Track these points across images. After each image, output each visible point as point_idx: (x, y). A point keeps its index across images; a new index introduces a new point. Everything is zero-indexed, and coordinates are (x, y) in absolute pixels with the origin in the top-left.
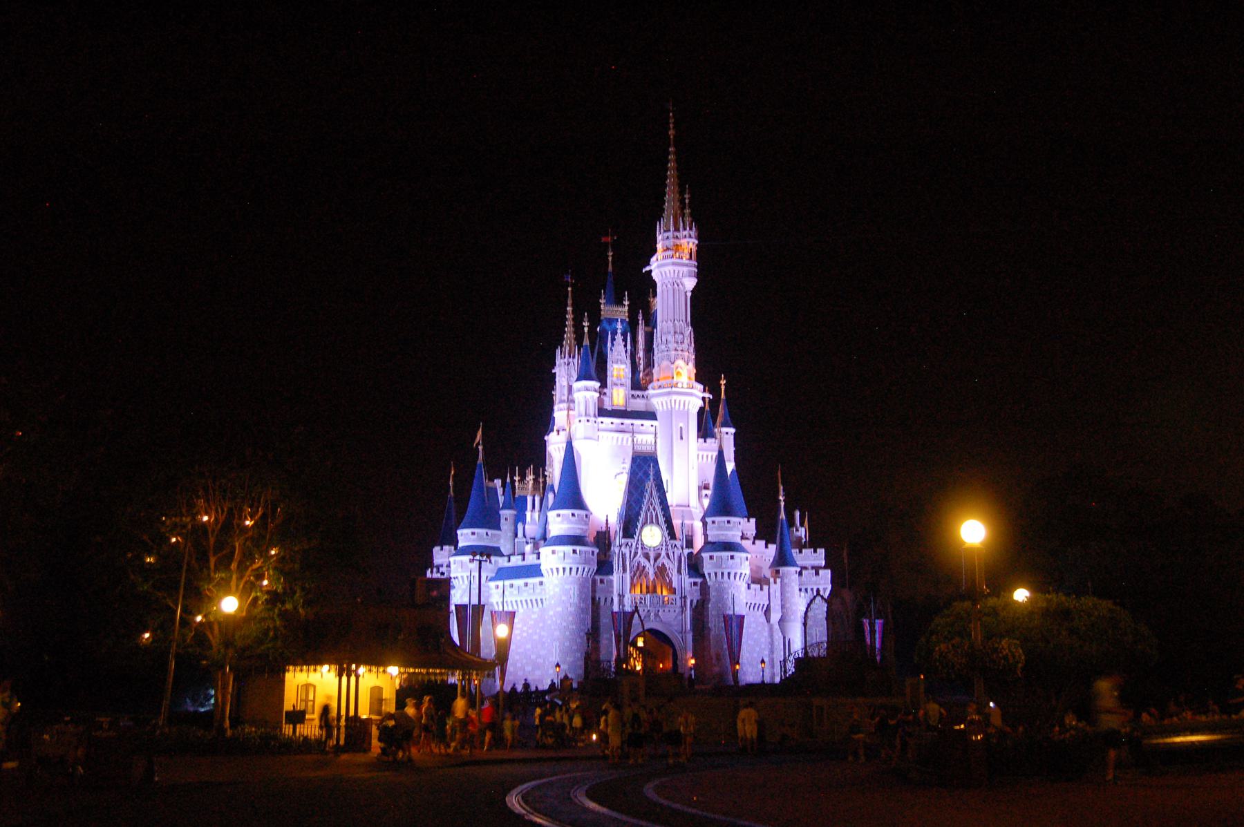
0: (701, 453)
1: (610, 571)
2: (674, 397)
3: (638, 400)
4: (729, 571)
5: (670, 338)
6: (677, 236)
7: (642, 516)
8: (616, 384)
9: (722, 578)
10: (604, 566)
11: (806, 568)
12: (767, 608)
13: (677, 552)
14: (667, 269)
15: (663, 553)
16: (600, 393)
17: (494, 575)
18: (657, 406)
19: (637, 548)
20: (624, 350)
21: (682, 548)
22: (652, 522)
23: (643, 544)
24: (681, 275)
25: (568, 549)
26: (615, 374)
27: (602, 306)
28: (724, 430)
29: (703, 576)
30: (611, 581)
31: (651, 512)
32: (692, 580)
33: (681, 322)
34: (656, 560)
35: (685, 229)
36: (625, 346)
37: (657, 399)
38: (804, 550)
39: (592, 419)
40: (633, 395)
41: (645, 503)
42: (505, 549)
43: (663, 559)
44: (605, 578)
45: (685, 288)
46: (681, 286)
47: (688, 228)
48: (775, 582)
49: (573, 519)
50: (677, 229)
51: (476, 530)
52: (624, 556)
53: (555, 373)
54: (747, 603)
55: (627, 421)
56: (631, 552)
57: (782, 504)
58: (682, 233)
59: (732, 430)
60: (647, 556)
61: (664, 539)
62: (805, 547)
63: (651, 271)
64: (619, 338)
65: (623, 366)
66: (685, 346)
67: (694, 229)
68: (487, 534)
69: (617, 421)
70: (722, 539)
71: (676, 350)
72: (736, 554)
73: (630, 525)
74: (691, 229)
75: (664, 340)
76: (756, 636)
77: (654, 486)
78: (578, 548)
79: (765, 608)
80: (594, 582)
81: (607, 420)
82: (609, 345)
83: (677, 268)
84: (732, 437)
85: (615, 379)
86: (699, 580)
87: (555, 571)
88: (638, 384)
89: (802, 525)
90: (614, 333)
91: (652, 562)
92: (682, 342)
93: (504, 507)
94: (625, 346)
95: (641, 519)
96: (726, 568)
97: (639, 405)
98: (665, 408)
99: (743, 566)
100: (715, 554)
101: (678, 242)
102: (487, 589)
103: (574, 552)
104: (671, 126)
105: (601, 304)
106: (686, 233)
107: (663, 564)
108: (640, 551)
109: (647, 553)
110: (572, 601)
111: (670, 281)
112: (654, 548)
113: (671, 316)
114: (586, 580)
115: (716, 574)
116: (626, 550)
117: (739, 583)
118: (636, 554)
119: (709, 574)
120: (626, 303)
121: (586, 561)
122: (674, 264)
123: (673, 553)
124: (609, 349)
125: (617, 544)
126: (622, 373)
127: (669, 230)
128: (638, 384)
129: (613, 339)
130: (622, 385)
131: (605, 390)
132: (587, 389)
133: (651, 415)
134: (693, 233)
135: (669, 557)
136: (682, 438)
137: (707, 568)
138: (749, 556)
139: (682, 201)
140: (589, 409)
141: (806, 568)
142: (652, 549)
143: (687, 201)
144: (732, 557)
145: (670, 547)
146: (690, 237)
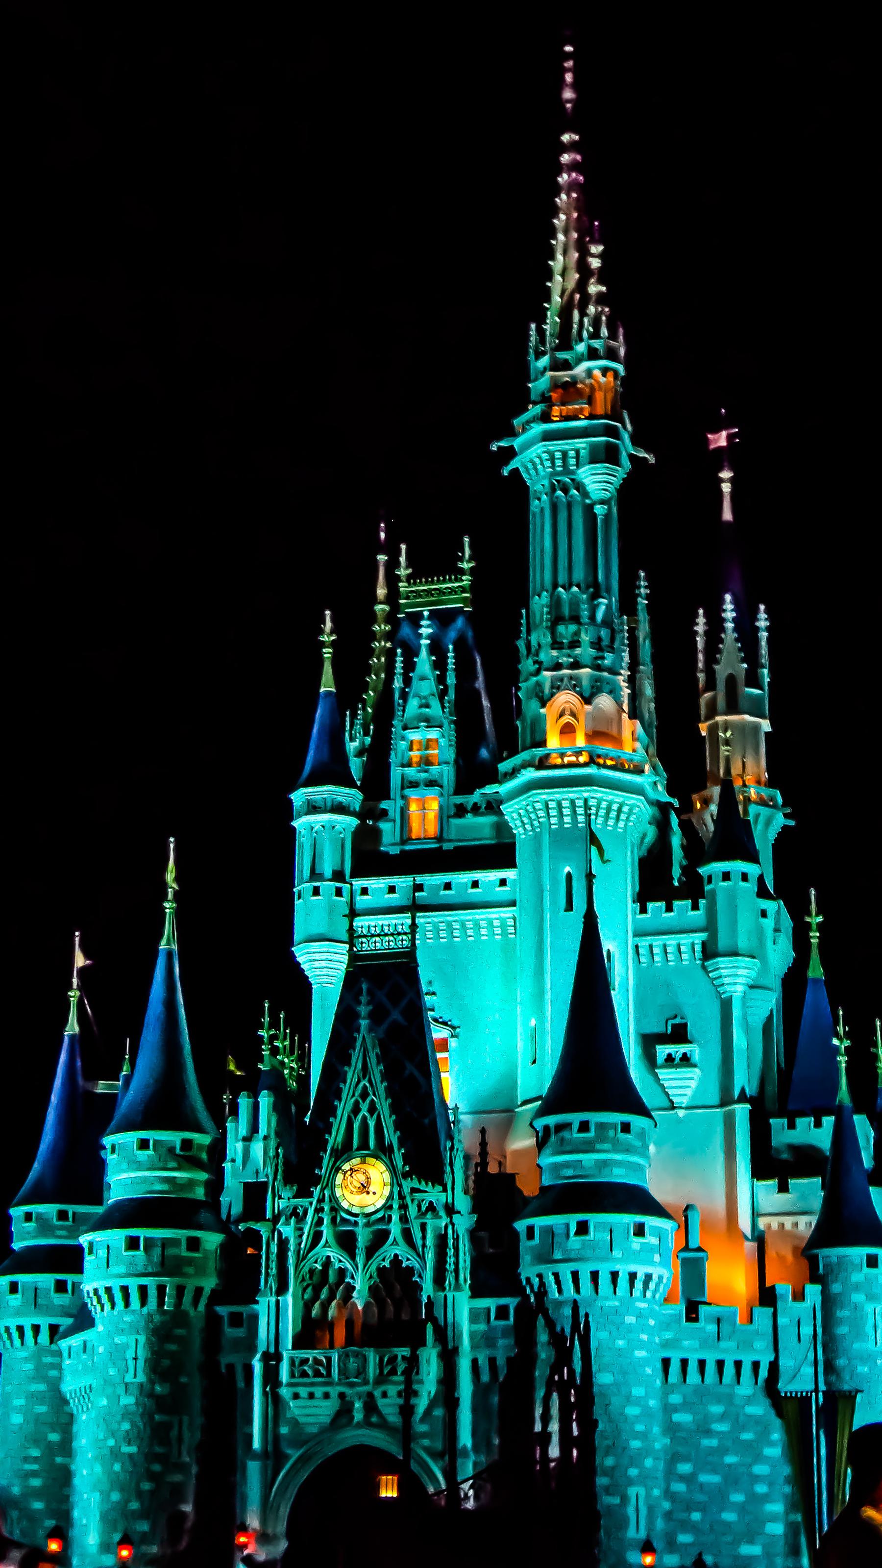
0: (644, 942)
1: (250, 1295)
2: (543, 795)
8: (414, 785)
9: (560, 1291)
12: (770, 1371)
15: (395, 1229)
17: (69, 1321)
23: (336, 1209)
24: (573, 461)
25: (117, 1236)
30: (255, 1318)
32: (490, 1303)
33: (575, 589)
34: (371, 1251)
39: (328, 887)
45: (585, 494)
46: (574, 492)
48: (799, 1296)
49: (144, 1155)
52: (283, 1244)
54: (666, 1362)
55: (432, 880)
56: (301, 1236)
60: (347, 1242)
61: (396, 1190)
65: (433, 734)
69: (403, 882)
71: (558, 667)
72: (594, 1219)
74: (613, 336)
76: (730, 1459)
79: (763, 1373)
80: (213, 1321)
81: (377, 884)
82: (398, 684)
85: (412, 772)
86: (512, 1302)
91: (360, 1259)
92: (575, 644)
94: (441, 680)
95: (335, 1138)
99: (617, 1253)
101: (564, 376)
102: (55, 1360)
103: (133, 1243)
104: (569, 77)
106: (581, 348)
107: (396, 1261)
108: (326, 1230)
110: (129, 1378)
111: (546, 482)
112: (368, 1215)
116: (287, 1230)
122: (548, 437)
123: (423, 1227)
125: (269, 1215)
129: (409, 666)
131: (384, 805)
132: (313, 808)
140: (322, 856)
142: (361, 1221)
145: (413, 1211)
146: (593, 354)
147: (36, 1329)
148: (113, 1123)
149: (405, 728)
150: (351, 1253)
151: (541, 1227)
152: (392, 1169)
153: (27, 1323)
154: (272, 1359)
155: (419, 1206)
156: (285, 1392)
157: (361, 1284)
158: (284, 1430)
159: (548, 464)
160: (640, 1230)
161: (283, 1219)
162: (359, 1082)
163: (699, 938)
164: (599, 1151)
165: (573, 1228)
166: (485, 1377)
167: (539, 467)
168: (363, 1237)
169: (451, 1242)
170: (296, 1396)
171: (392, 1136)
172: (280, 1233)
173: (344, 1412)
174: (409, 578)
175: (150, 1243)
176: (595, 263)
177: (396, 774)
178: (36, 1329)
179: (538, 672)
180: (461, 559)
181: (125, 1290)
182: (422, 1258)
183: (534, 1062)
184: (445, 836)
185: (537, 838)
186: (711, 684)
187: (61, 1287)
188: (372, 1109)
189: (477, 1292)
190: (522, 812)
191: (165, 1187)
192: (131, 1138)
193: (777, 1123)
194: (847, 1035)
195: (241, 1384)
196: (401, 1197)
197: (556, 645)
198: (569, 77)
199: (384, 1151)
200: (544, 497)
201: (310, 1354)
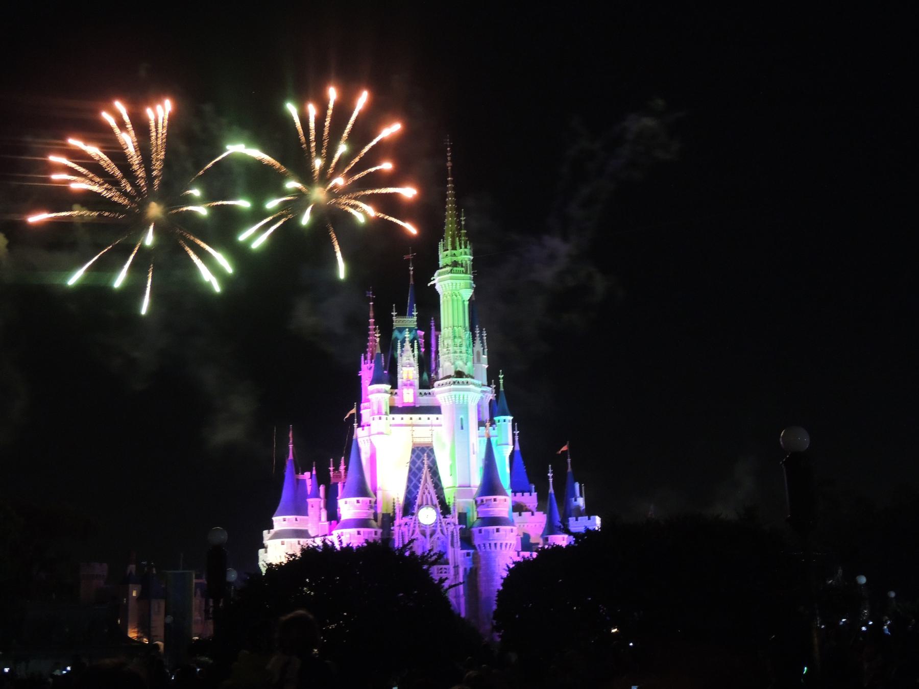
3: (425, 397)
4: (495, 542)
5: (450, 342)
6: (454, 254)
7: (418, 498)
13: (451, 528)
14: (446, 282)
15: (439, 529)
16: (391, 393)
18: (440, 401)
20: (412, 354)
21: (455, 525)
22: (427, 504)
23: (419, 523)
26: (405, 376)
27: (394, 318)
28: (502, 418)
29: (474, 547)
31: (427, 495)
32: (465, 551)
34: (431, 536)
35: (461, 248)
36: (413, 351)
37: (442, 394)
38: (579, 518)
40: (421, 394)
41: (421, 488)
42: (312, 533)
43: (438, 534)
45: (462, 298)
47: (463, 247)
50: (454, 248)
51: (287, 517)
53: (361, 376)
56: (409, 531)
57: (551, 480)
58: (458, 251)
59: (510, 418)
61: (438, 517)
62: (581, 515)
63: (434, 285)
64: (407, 345)
65: (412, 368)
66: (464, 349)
67: (469, 247)
68: (296, 520)
71: (455, 352)
73: (409, 507)
74: (466, 247)
75: (446, 344)
77: (428, 472)
78: (362, 530)
81: (398, 417)
82: (399, 351)
83: (454, 281)
84: (510, 424)
86: (471, 551)
88: (426, 384)
89: (581, 496)
90: (403, 341)
92: (461, 346)
93: (311, 497)
94: (413, 351)
95: (418, 501)
96: (492, 540)
97: (424, 401)
98: (461, 401)
99: (507, 538)
101: (455, 259)
104: (449, 158)
105: (392, 316)
106: (462, 250)
109: (424, 531)
111: (450, 292)
113: (451, 324)
115: (484, 545)
116: (404, 529)
117: (505, 552)
118: (414, 531)
119: (479, 545)
120: (415, 313)
122: (451, 278)
124: (399, 356)
127: (448, 250)
128: (426, 384)
129: (402, 346)
130: (411, 385)
131: (396, 391)
132: (379, 391)
133: (435, 410)
134: (468, 250)
135: (443, 534)
136: (462, 428)
137: (476, 542)
138: (514, 528)
139: (459, 223)
143: (463, 223)
144: (498, 530)
145: (444, 524)
146: (466, 254)
149: (402, 366)
150: (425, 537)
151: (485, 530)
155: (445, 523)
159: (451, 287)
160: (512, 531)
161: (403, 526)
162: (425, 484)
164: (500, 507)
165: (495, 531)
167: (447, 287)
168: (428, 533)
169: (455, 534)
172: (402, 531)
174: (396, 315)
176: (463, 223)
177: (400, 382)
179: (448, 353)
180: (413, 311)
182: (447, 538)
183: (451, 475)
184: (416, 403)
188: (429, 493)
190: (446, 398)
191: (365, 515)
194: (552, 472)
196: (440, 520)
197: (455, 345)
198: (449, 158)
200: (449, 297)
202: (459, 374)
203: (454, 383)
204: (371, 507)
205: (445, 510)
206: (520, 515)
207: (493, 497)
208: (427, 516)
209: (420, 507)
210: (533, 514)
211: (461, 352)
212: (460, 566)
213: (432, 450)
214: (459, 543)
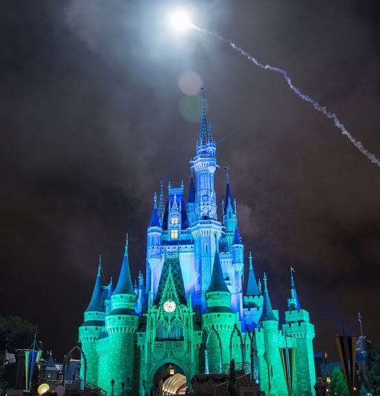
1: (144, 331)
2: (201, 229)
10: (142, 326)
11: (294, 322)
13: (186, 314)
15: (177, 316)
19: (160, 314)
21: (189, 312)
25: (116, 317)
26: (173, 222)
27: (169, 189)
30: (145, 335)
32: (198, 332)
36: (179, 207)
37: (197, 231)
39: (156, 247)
44: (142, 333)
48: (259, 331)
55: (177, 247)
62: (294, 309)
64: (175, 202)
70: (215, 305)
71: (204, 205)
72: (221, 314)
78: (121, 316)
87: (116, 331)
88: (185, 224)
91: (169, 322)
94: (179, 207)
95: (163, 296)
97: (183, 237)
100: (209, 315)
101: (204, 150)
103: (119, 318)
108: (162, 316)
114: (129, 334)
116: (153, 315)
121: (127, 323)
122: (201, 161)
126: (177, 222)
129: (172, 204)
132: (153, 231)
137: (205, 325)
141: (294, 322)
144: (219, 316)
146: (211, 146)
147: (91, 338)
148: (91, 303)
152: (176, 304)
153: (89, 337)
154: (150, 343)
156: (152, 351)
157: (169, 328)
158: (152, 359)
160: (230, 316)
163: (231, 260)
166: (196, 347)
170: (155, 352)
171: (176, 296)
173: (166, 356)
175: (123, 318)
177: (169, 225)
178: (91, 338)
181: (113, 328)
185: (200, 239)
186: (226, 213)
187: (97, 329)
189: (194, 330)
192: (118, 296)
193: (246, 298)
195: (141, 349)
199: (174, 299)
201: (159, 342)
202: (206, 218)
203: (201, 223)
204: (132, 301)
205: (183, 300)
206: (249, 310)
207: (217, 292)
208: (170, 307)
209: (166, 299)
210: (258, 309)
211: (207, 204)
212: (192, 342)
213: (178, 264)
214: (192, 325)
